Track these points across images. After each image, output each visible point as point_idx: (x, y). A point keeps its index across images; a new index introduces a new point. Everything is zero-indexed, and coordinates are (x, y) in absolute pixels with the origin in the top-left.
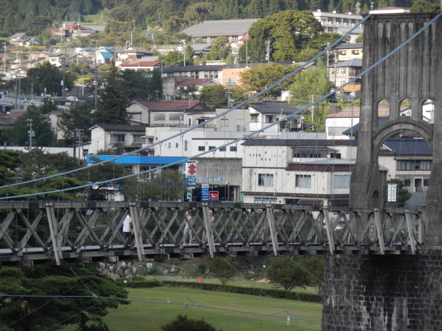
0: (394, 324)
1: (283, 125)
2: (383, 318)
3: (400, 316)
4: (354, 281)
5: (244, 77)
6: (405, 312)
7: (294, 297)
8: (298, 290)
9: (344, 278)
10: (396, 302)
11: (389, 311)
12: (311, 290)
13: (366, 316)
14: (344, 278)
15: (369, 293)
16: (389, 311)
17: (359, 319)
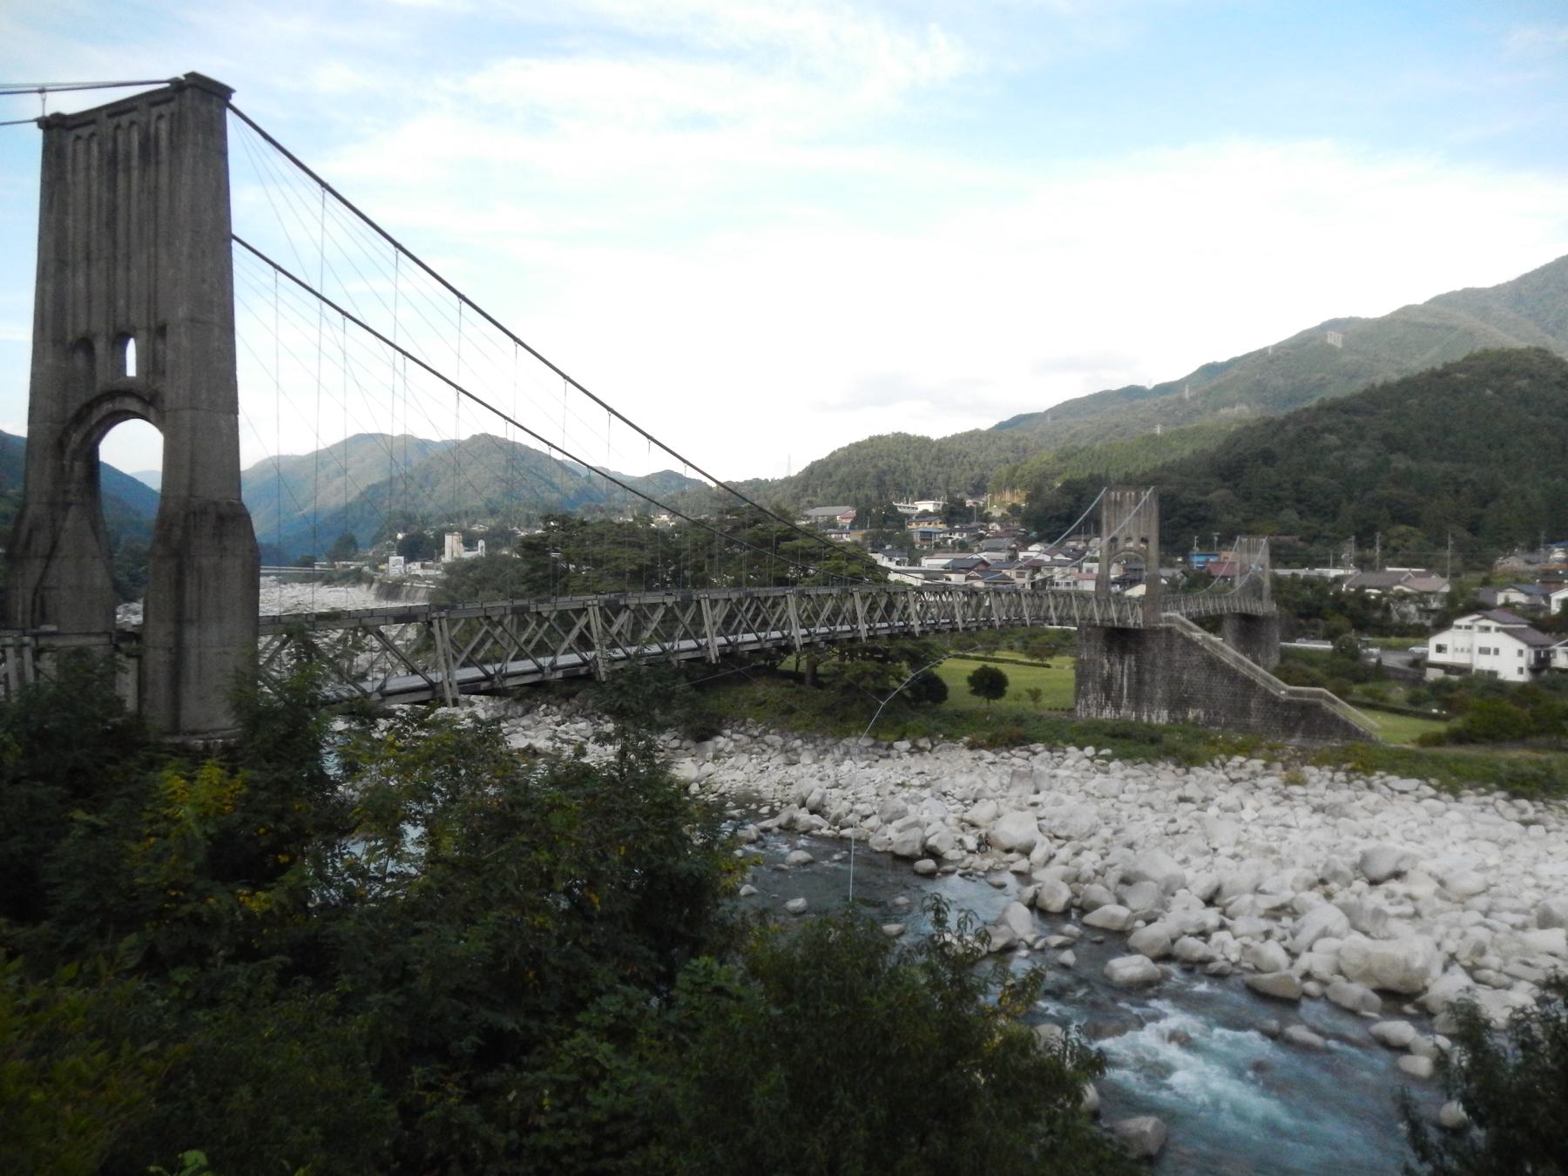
0: (1126, 671)
1: (898, 563)
2: (1118, 667)
3: (1130, 665)
4: (1099, 644)
5: (865, 537)
6: (1133, 663)
7: (968, 658)
8: (972, 655)
9: (1092, 643)
10: (1127, 657)
11: (1122, 664)
12: (976, 655)
13: (1107, 666)
14: (1092, 643)
15: (1110, 651)
16: (1122, 664)
17: (1102, 667)
